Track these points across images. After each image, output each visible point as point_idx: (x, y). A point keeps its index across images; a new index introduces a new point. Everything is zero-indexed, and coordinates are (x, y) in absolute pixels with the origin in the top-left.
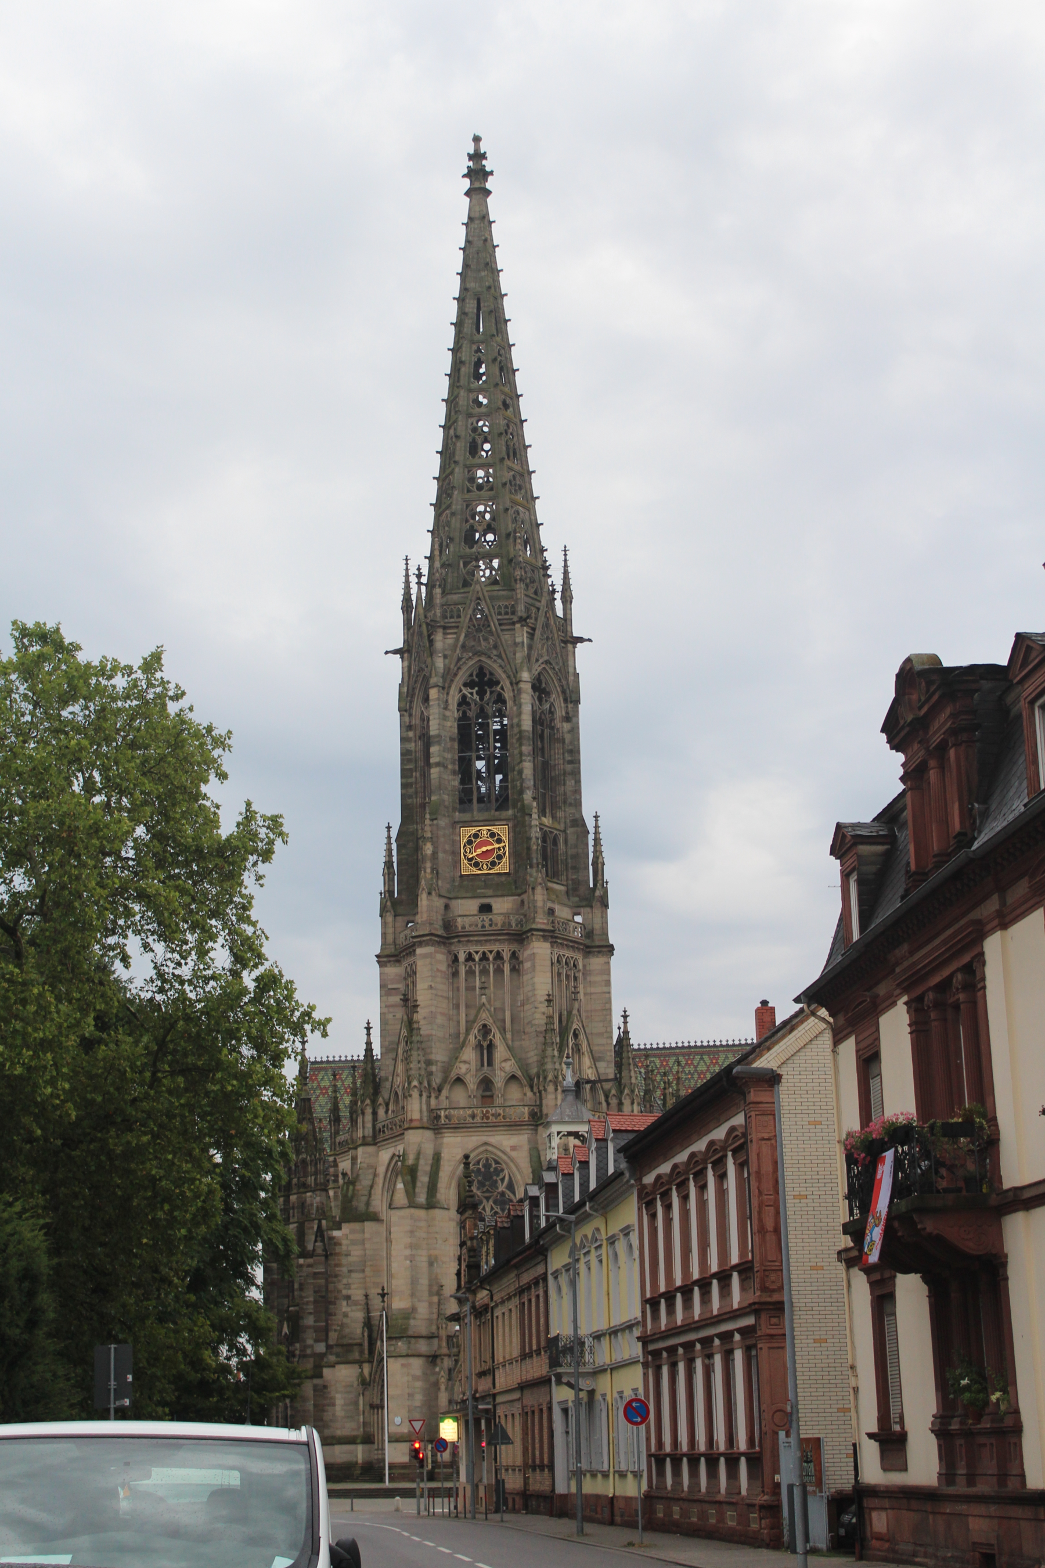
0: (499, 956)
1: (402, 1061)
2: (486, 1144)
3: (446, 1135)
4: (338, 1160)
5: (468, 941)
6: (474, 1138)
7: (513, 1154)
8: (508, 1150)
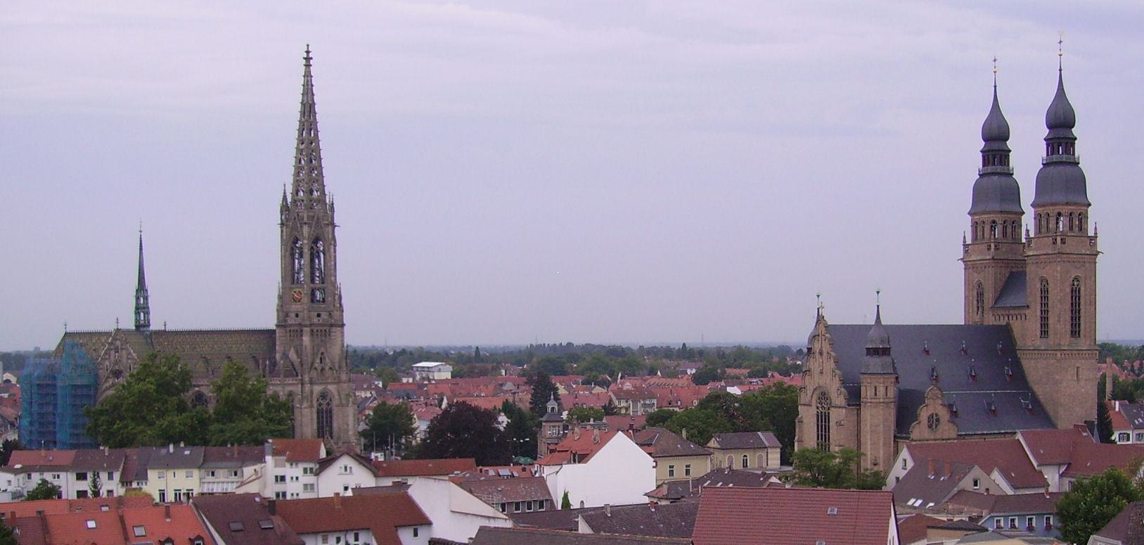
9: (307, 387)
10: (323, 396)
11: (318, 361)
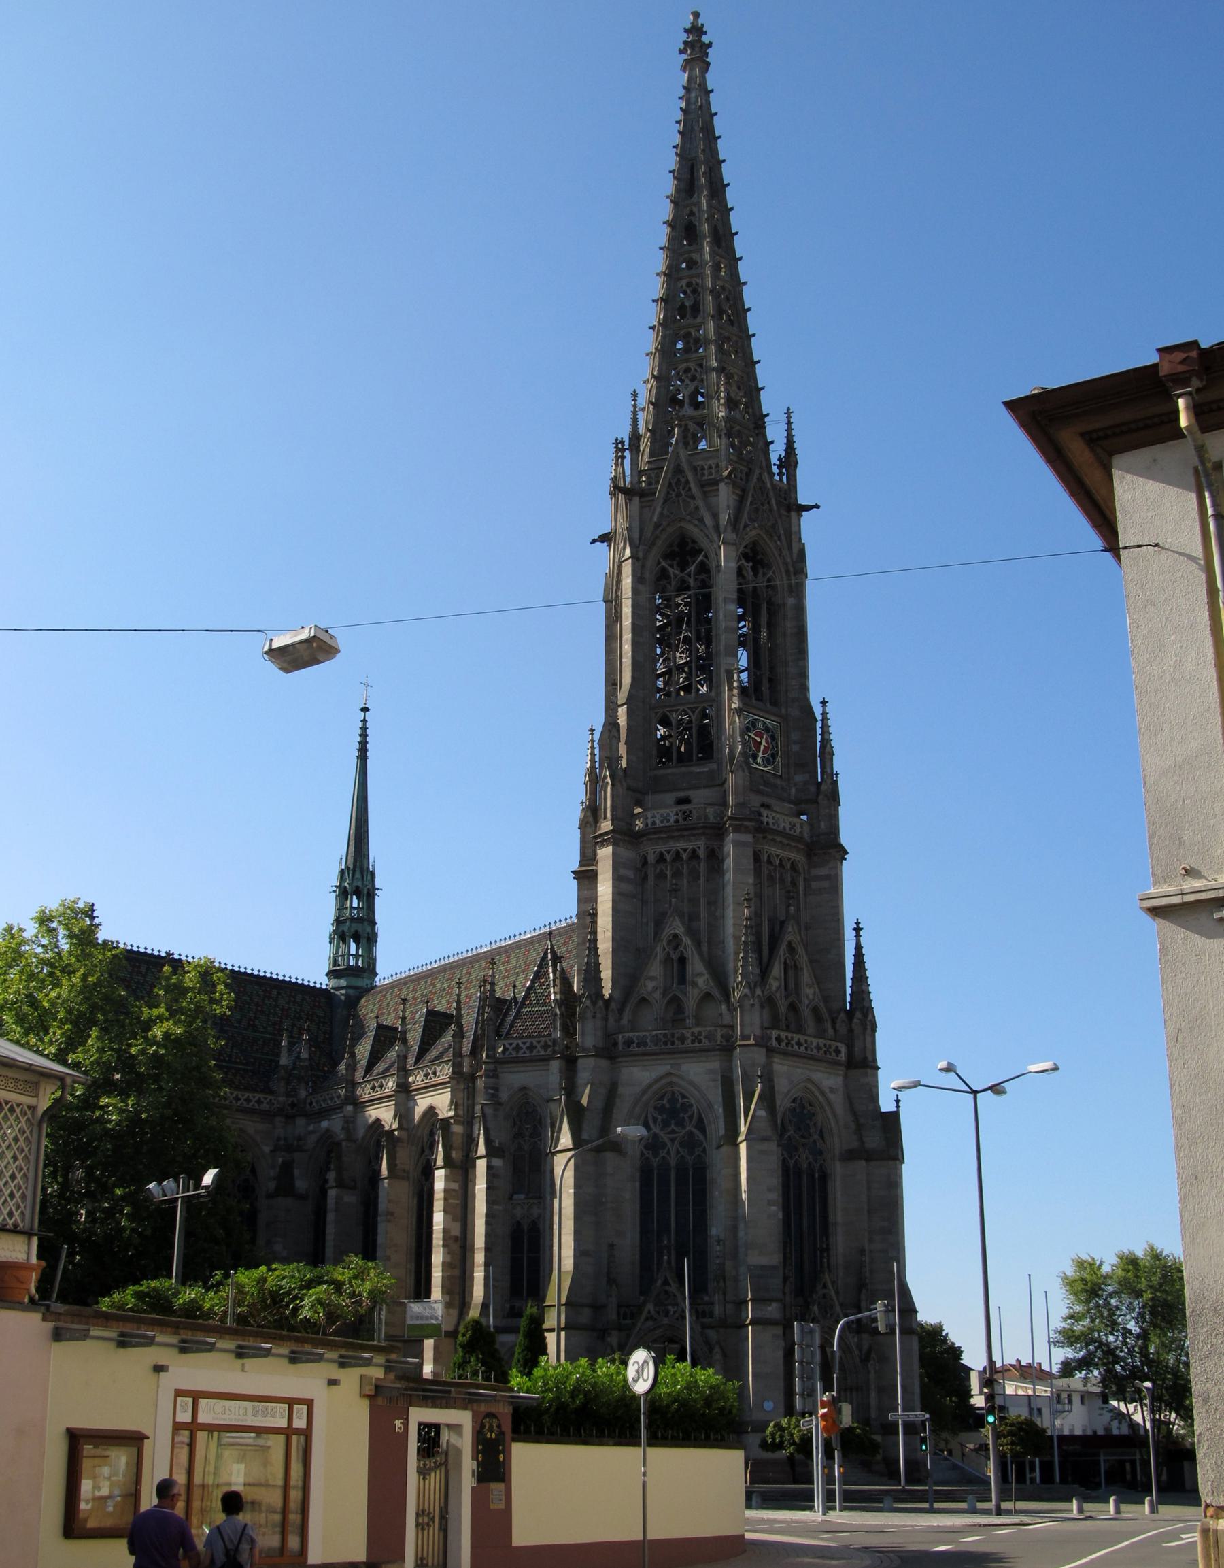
1: (660, 961)
2: (809, 1080)
3: (776, 1060)
4: (499, 1070)
5: (773, 840)
6: (799, 1071)
7: (832, 1097)
8: (827, 1091)
9: (587, 1068)
11: (656, 969)
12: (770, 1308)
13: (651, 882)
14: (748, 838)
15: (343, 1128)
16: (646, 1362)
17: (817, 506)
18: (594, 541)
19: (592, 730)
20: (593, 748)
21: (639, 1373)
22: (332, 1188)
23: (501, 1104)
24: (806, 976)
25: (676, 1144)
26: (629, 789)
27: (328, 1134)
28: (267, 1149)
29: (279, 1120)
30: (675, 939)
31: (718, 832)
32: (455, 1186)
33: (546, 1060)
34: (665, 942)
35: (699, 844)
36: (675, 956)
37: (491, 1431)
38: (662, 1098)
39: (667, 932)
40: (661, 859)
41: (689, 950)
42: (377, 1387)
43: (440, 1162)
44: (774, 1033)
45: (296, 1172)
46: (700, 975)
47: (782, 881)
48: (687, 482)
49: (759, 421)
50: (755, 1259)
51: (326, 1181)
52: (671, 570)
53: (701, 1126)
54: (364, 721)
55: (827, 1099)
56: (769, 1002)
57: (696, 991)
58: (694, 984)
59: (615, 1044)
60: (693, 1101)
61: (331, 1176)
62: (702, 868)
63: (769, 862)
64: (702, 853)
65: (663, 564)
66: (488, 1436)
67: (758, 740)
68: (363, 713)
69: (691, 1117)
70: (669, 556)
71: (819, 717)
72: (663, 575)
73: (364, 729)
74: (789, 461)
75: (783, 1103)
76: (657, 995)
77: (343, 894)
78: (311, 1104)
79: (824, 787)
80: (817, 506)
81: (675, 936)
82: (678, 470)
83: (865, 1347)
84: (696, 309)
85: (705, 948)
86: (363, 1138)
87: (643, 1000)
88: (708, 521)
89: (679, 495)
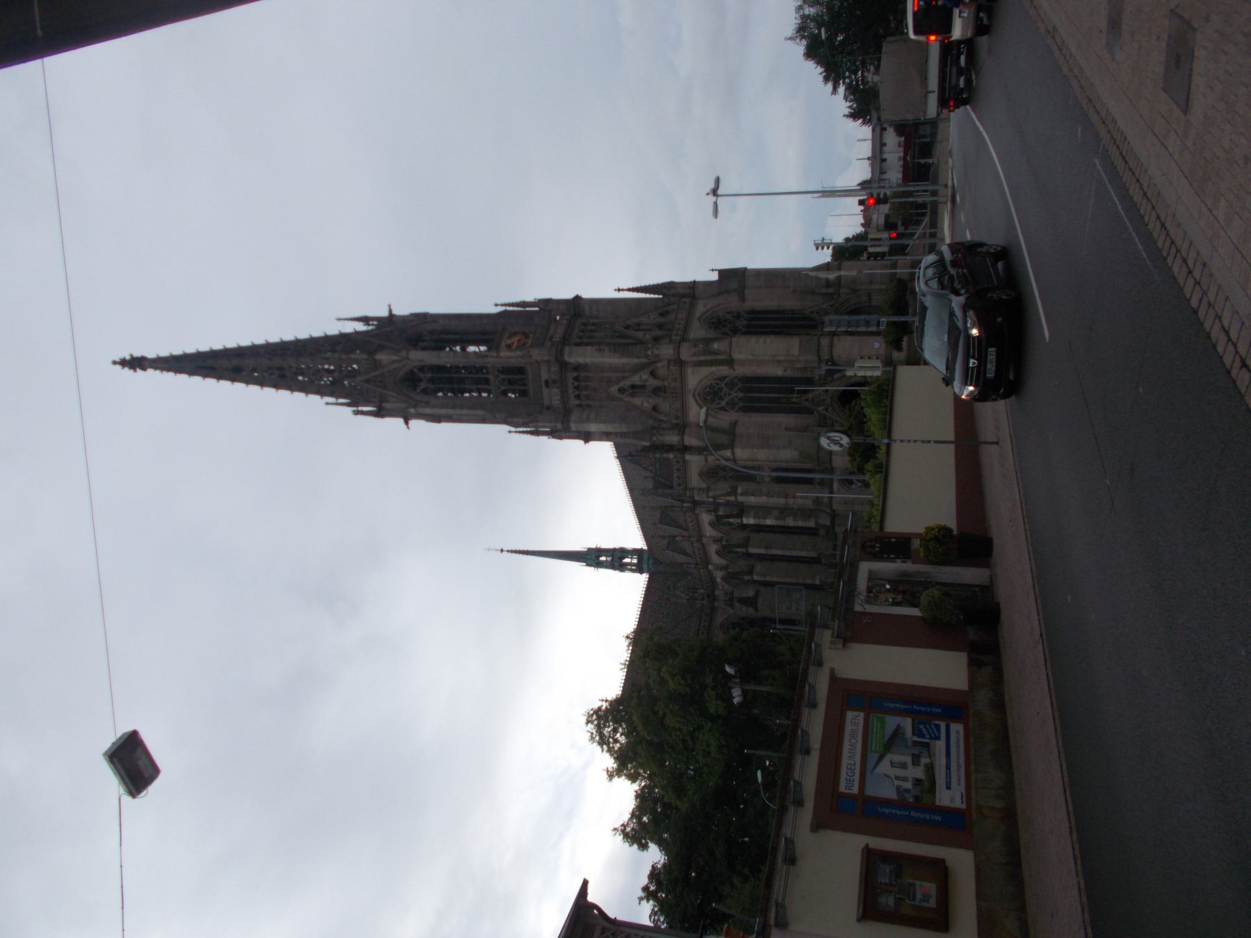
0: (585, 324)
2: (699, 319)
7: (709, 306)
9: (690, 441)
10: (711, 395)
11: (637, 401)
12: (823, 343)
13: (590, 402)
14: (567, 349)
15: (721, 570)
16: (828, 438)
17: (389, 306)
18: (408, 428)
19: (510, 432)
20: (520, 432)
21: (836, 443)
22: (752, 578)
23: (708, 488)
24: (644, 320)
25: (731, 392)
26: (540, 413)
27: (724, 579)
28: (731, 611)
29: (716, 604)
30: (621, 390)
31: (564, 365)
32: (752, 513)
33: (685, 461)
34: (622, 396)
35: (571, 375)
36: (631, 391)
37: (874, 547)
38: (706, 399)
39: (617, 394)
40: (578, 397)
41: (626, 383)
42: (837, 637)
43: (739, 521)
44: (674, 338)
45: (744, 595)
46: (640, 377)
47: (592, 331)
48: (375, 376)
49: (343, 337)
50: (795, 351)
51: (748, 581)
52: (422, 387)
53: (722, 379)
54: (508, 551)
55: (709, 310)
56: (656, 339)
57: (650, 380)
58: (646, 380)
59: (678, 424)
60: (709, 383)
61: (746, 578)
62: (583, 374)
63: (580, 338)
64: (575, 374)
65: (419, 391)
66: (877, 549)
67: (516, 342)
68: (504, 552)
69: (717, 384)
70: (415, 388)
71: (503, 308)
72: (425, 391)
73: (512, 552)
74: (365, 320)
75: (711, 334)
76: (651, 401)
77: (599, 565)
78: (708, 587)
79: (542, 306)
80: (389, 306)
81: (619, 390)
82: (367, 381)
83: (847, 291)
84: (281, 369)
85: (626, 374)
86: (725, 559)
87: (655, 408)
88: (395, 366)
89: (381, 381)
